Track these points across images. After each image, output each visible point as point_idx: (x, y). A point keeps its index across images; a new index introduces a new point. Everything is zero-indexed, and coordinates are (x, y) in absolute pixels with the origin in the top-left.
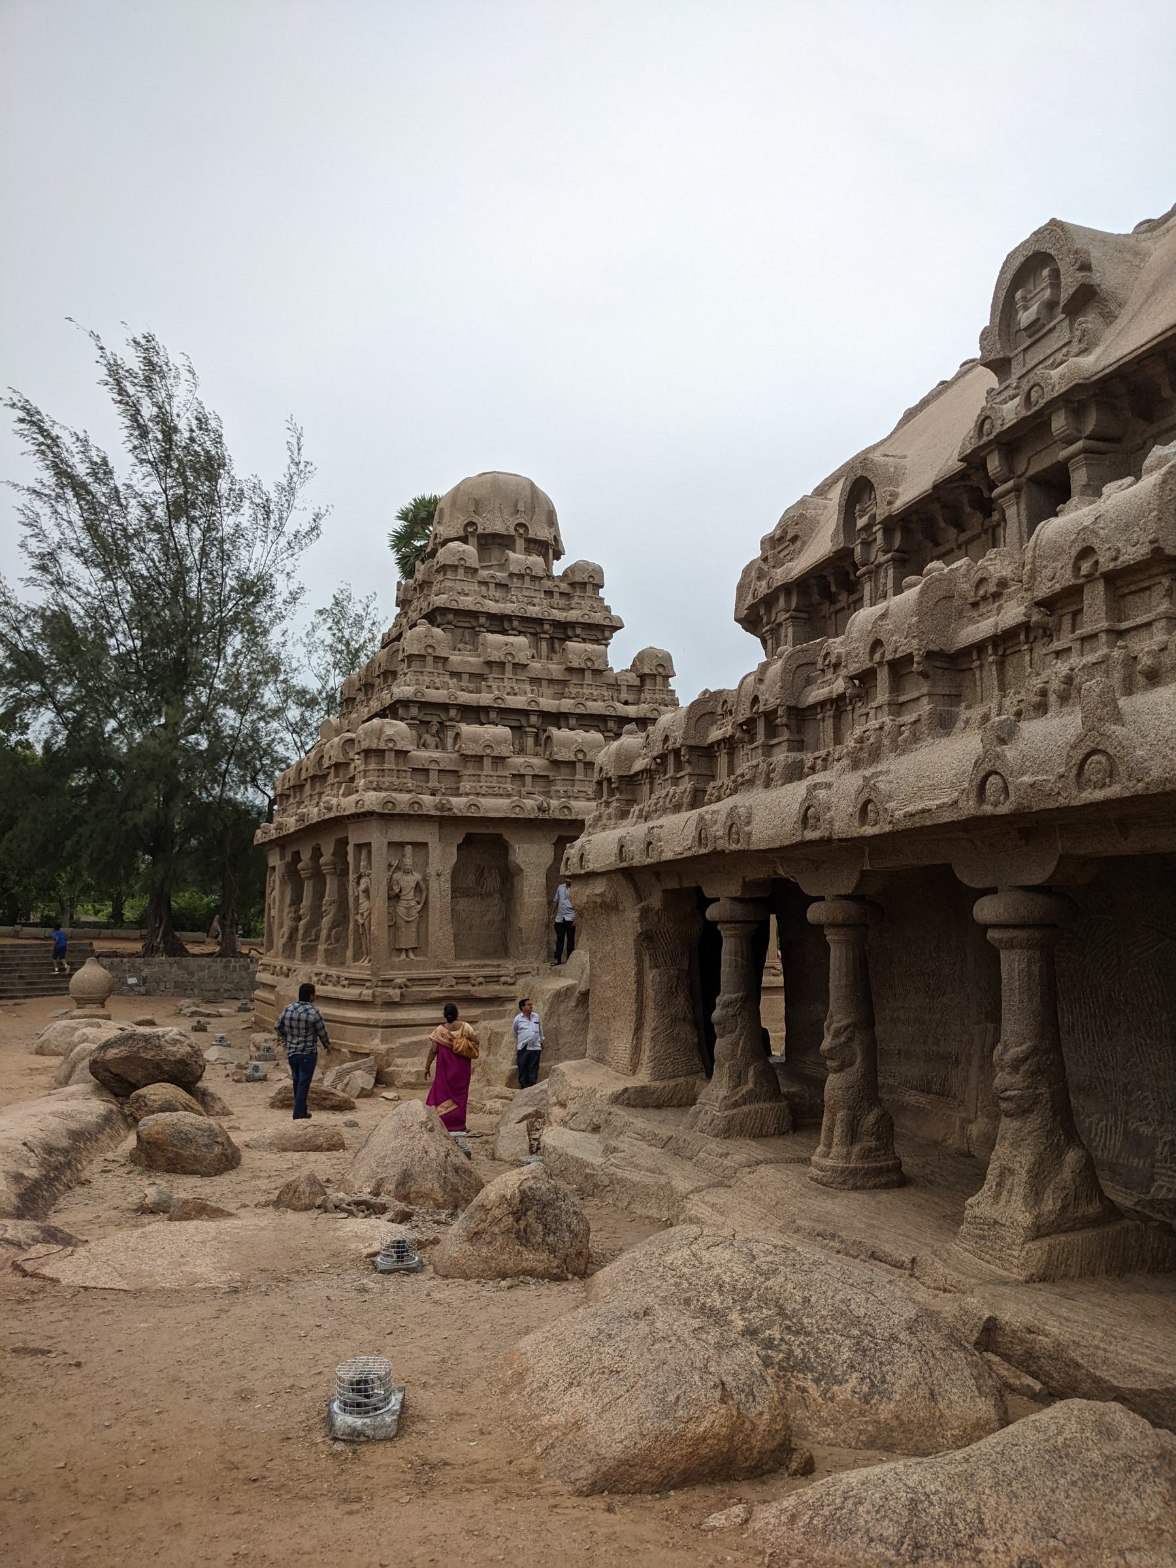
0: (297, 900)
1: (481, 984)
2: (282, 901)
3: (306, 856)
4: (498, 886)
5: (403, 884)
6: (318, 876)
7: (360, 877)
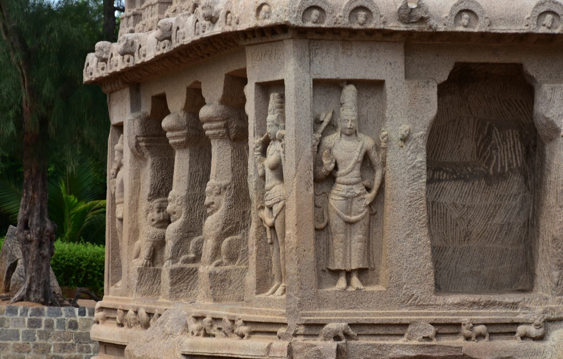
0: (161, 189)
1: (480, 336)
2: (136, 188)
3: (177, 104)
4: (518, 161)
5: (339, 154)
6: (198, 144)
7: (266, 143)
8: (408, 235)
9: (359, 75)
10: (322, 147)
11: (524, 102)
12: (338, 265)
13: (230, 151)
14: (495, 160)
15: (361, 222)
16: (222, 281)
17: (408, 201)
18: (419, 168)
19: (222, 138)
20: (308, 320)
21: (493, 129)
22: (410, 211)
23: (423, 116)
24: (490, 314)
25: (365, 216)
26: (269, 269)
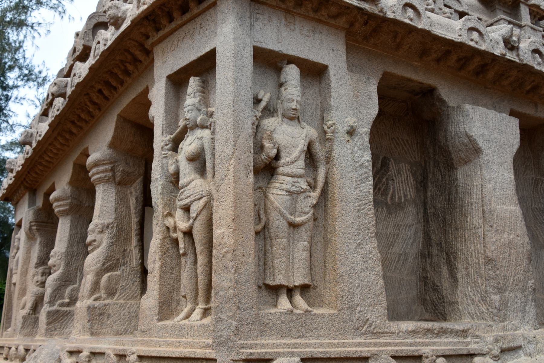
2: (27, 260)
4: (411, 194)
8: (359, 245)
9: (303, 55)
10: (260, 130)
11: (409, 142)
12: (280, 279)
13: (114, 194)
14: (391, 191)
15: (307, 226)
16: (101, 314)
17: (357, 204)
18: (366, 167)
19: (108, 181)
20: (251, 354)
21: (390, 161)
22: (359, 217)
23: (367, 113)
24: (445, 344)
25: (310, 218)
26: (175, 289)
